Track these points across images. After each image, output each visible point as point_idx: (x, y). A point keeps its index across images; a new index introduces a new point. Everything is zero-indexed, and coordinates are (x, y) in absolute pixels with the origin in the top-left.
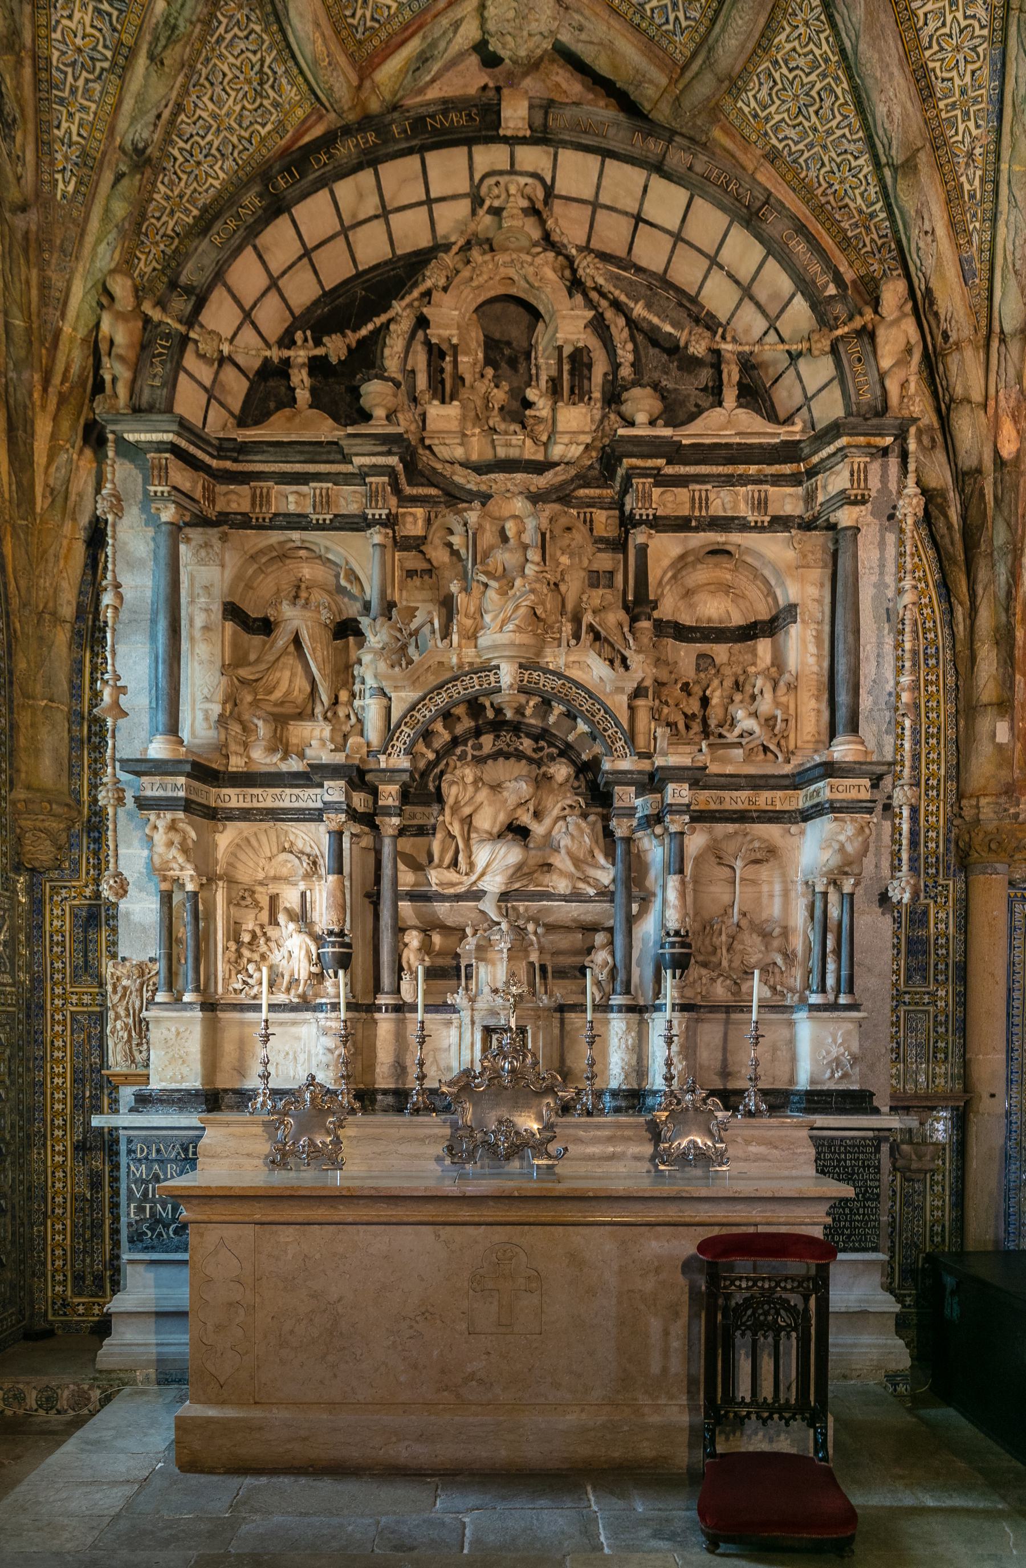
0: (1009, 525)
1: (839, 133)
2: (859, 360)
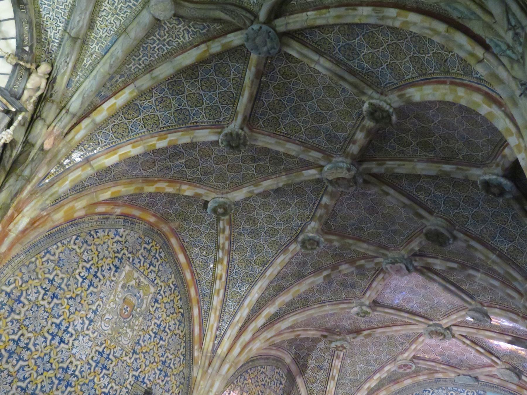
0: (31, 170)
1: (60, 11)
2: (21, 77)
